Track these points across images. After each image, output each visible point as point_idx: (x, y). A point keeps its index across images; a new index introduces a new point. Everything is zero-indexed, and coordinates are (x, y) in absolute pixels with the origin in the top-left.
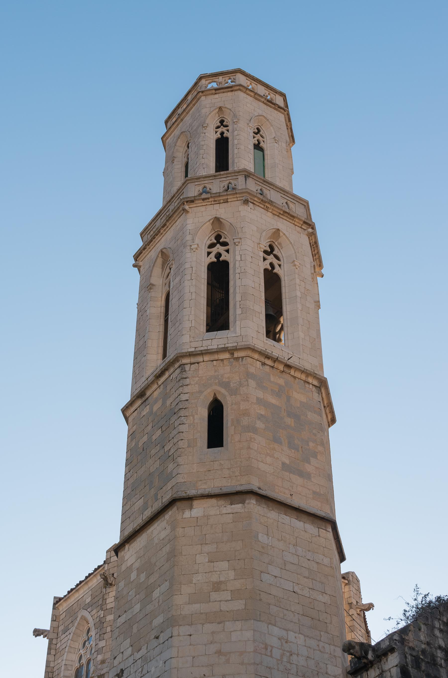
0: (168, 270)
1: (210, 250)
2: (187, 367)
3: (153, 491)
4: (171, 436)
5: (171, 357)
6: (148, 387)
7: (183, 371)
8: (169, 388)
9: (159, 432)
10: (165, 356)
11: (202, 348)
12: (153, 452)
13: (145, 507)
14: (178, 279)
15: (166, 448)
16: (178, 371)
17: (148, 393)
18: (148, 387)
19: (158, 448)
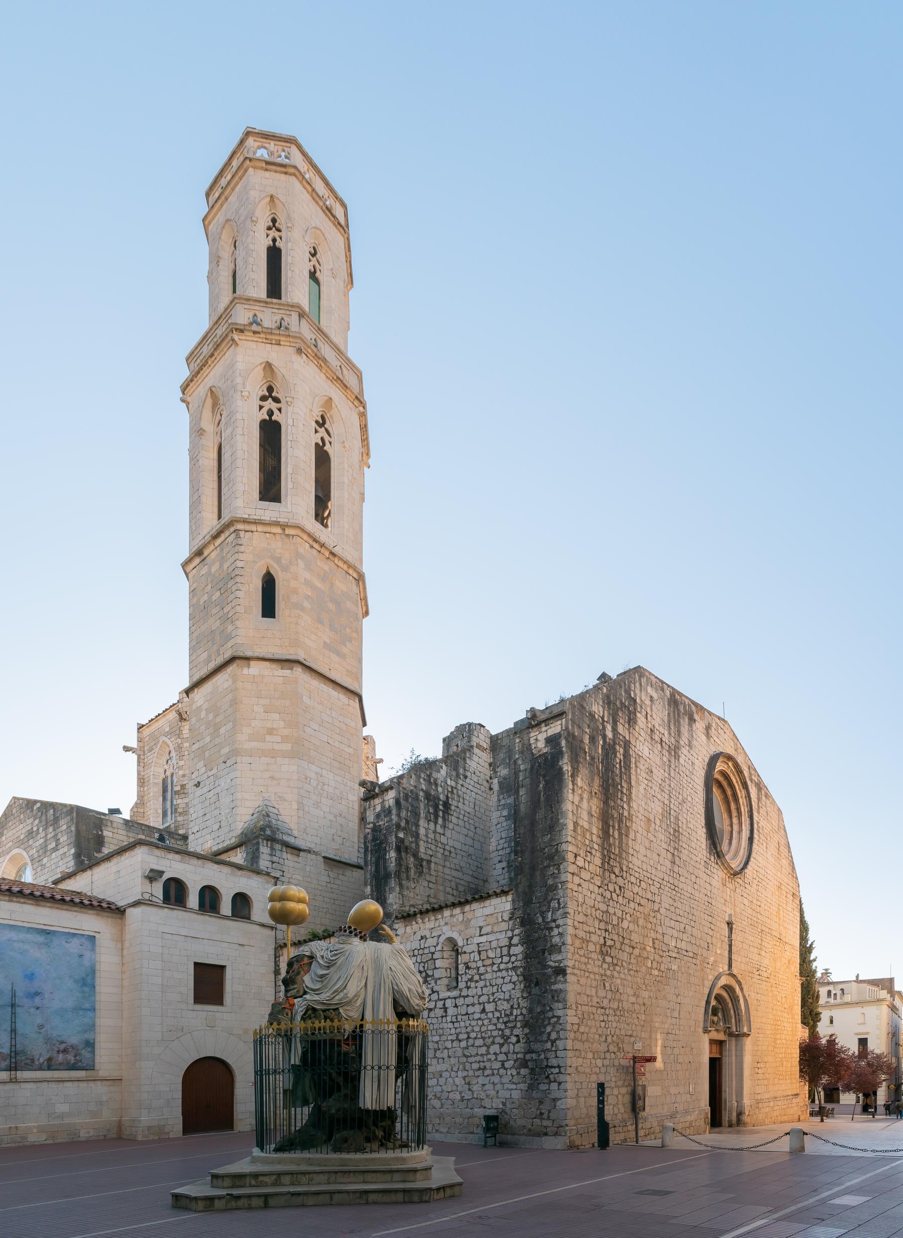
0: (218, 417)
1: (263, 403)
2: (242, 534)
3: (215, 647)
4: (230, 599)
5: (226, 519)
6: (205, 546)
7: (238, 537)
8: (225, 551)
9: (218, 594)
10: (220, 517)
11: (255, 517)
12: (214, 611)
13: (209, 660)
14: (229, 430)
15: (226, 610)
16: (233, 536)
17: (206, 553)
18: (205, 546)
19: (218, 608)
